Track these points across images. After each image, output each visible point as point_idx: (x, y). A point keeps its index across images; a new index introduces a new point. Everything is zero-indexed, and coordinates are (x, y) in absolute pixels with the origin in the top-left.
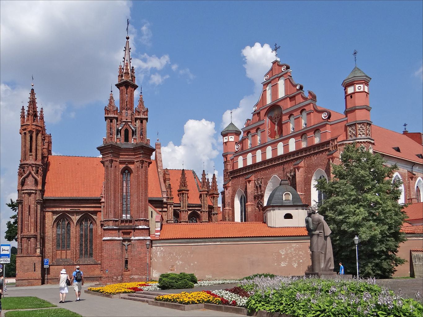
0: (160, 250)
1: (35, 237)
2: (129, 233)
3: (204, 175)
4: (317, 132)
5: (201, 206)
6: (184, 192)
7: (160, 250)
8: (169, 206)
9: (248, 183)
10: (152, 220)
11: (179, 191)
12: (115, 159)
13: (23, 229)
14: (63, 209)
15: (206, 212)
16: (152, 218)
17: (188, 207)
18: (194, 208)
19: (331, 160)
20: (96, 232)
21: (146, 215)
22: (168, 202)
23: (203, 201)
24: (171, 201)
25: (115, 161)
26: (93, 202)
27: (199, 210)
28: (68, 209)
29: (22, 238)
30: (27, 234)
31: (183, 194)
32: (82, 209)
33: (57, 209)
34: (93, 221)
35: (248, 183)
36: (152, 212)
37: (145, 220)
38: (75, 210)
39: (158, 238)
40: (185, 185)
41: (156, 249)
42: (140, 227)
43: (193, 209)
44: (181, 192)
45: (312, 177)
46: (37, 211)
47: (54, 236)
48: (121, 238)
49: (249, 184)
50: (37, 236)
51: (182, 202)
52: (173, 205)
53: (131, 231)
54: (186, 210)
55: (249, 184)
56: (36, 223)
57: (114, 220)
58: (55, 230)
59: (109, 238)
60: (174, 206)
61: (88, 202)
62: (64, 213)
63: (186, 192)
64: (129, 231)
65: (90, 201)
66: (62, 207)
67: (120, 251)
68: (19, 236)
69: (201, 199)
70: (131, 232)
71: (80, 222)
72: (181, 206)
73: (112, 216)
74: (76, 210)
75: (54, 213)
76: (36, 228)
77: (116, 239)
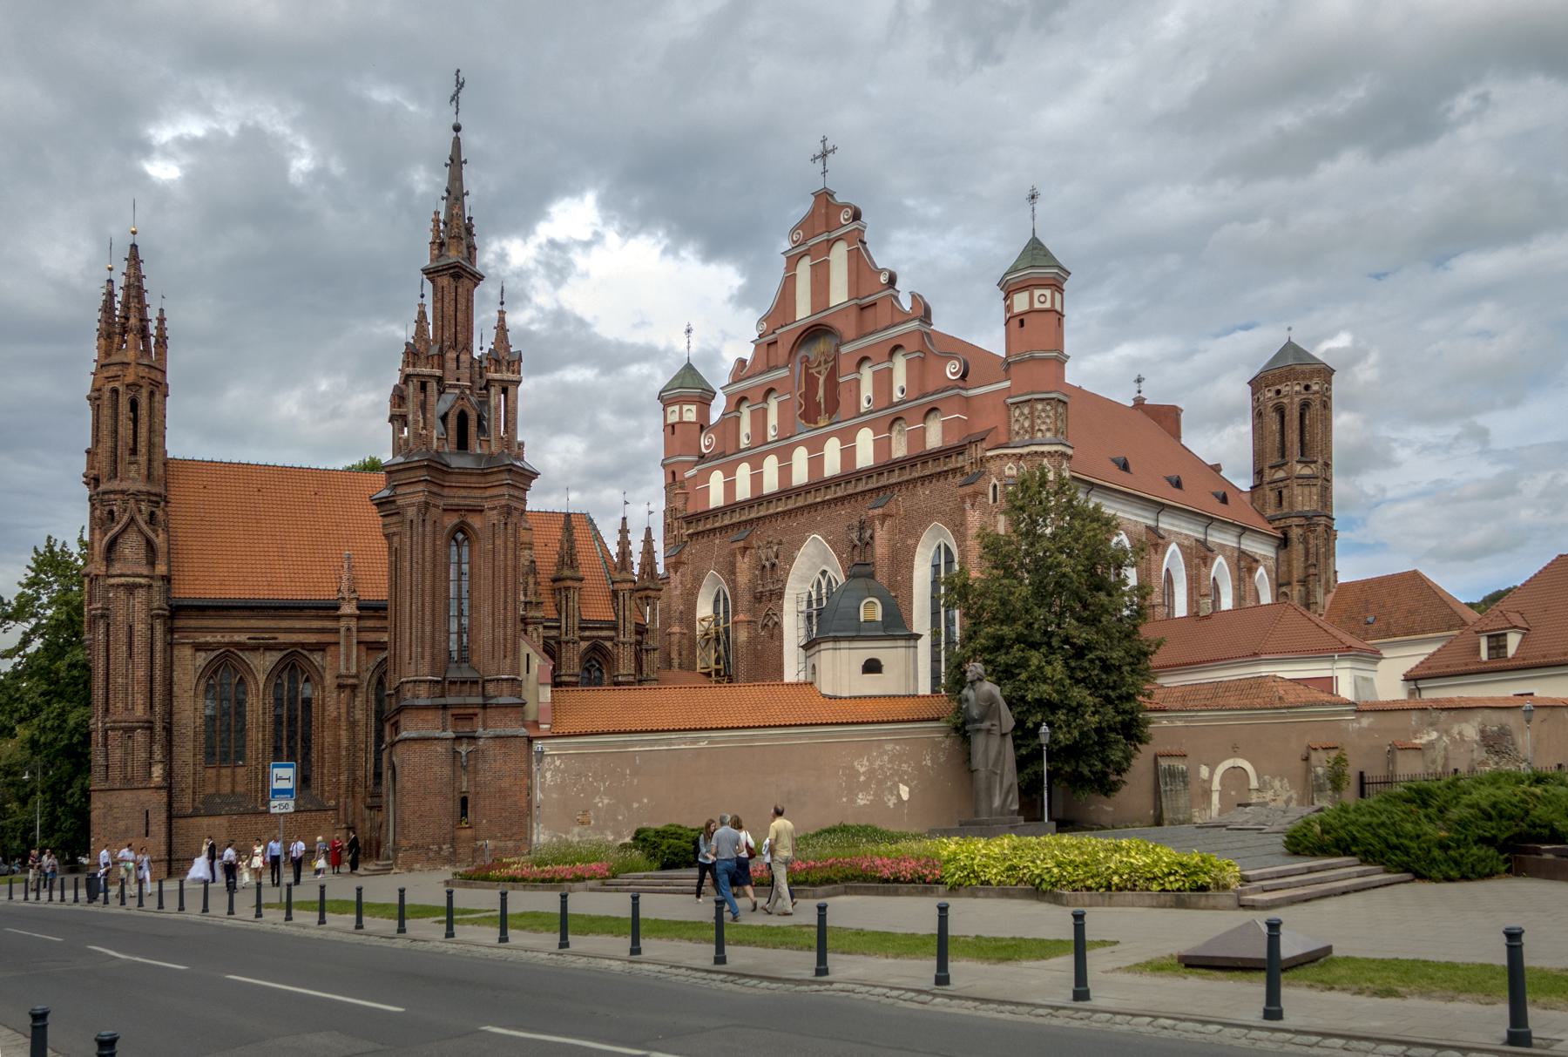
1: (149, 727)
2: (471, 717)
3: (624, 531)
4: (932, 416)
6: (569, 583)
8: (530, 628)
9: (739, 557)
10: (527, 679)
11: (554, 581)
13: (111, 702)
15: (631, 644)
17: (581, 629)
18: (595, 633)
19: (968, 501)
20: (324, 710)
21: (515, 668)
22: (530, 614)
23: (621, 613)
24: (539, 614)
26: (317, 616)
27: (610, 639)
28: (238, 638)
29: (106, 731)
30: (125, 716)
32: (283, 638)
33: (209, 638)
34: (314, 677)
35: (739, 557)
36: (528, 655)
37: (513, 680)
38: (263, 639)
42: (501, 701)
43: (594, 637)
44: (561, 584)
45: (915, 547)
47: (199, 721)
48: (452, 735)
49: (743, 557)
51: (564, 615)
52: (542, 623)
53: (477, 711)
54: (576, 638)
55: (743, 557)
56: (151, 682)
57: (431, 681)
58: (200, 705)
59: (413, 734)
60: (545, 627)
62: (228, 651)
63: (577, 584)
64: (471, 711)
65: (307, 613)
67: (447, 771)
68: (100, 725)
69: (615, 605)
70: (476, 715)
71: (275, 673)
73: (427, 669)
75: (198, 647)
77: (437, 735)
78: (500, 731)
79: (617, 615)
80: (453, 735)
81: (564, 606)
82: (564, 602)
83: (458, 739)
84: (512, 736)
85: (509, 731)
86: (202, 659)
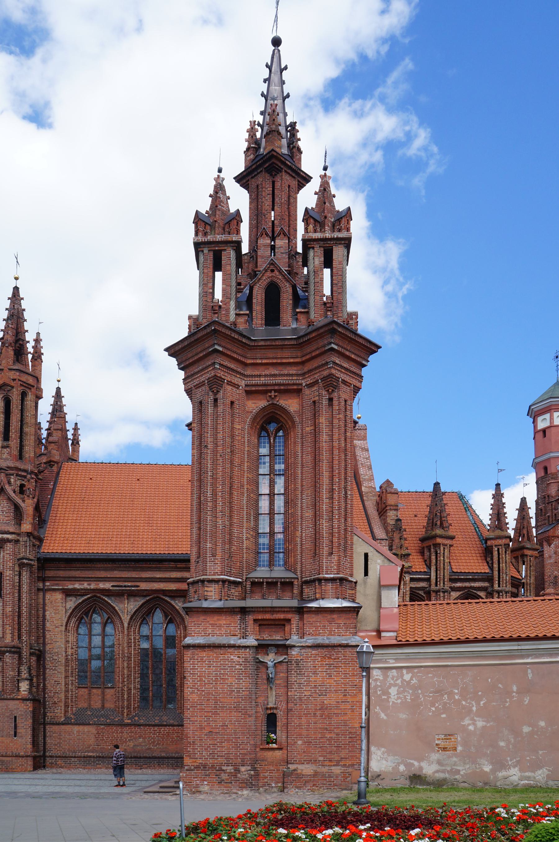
0: (399, 682)
2: (282, 624)
5: (489, 579)
7: (399, 682)
12: (228, 378)
14: (93, 586)
16: (366, 574)
23: (496, 566)
25: (230, 383)
26: (176, 568)
31: (437, 545)
33: (77, 586)
38: (125, 586)
39: (394, 642)
40: (441, 524)
41: (386, 676)
44: (430, 543)
46: (19, 586)
50: (20, 648)
53: (289, 616)
61: (160, 568)
64: (282, 616)
65: (166, 564)
66: (89, 579)
69: (489, 559)
70: (289, 621)
72: (430, 578)
74: (129, 586)
75: (68, 593)
76: (19, 630)
78: (320, 640)
79: (492, 568)
80: (255, 643)
81: (434, 561)
82: (433, 557)
83: (262, 647)
84: (340, 646)
85: (335, 640)
86: (72, 603)
